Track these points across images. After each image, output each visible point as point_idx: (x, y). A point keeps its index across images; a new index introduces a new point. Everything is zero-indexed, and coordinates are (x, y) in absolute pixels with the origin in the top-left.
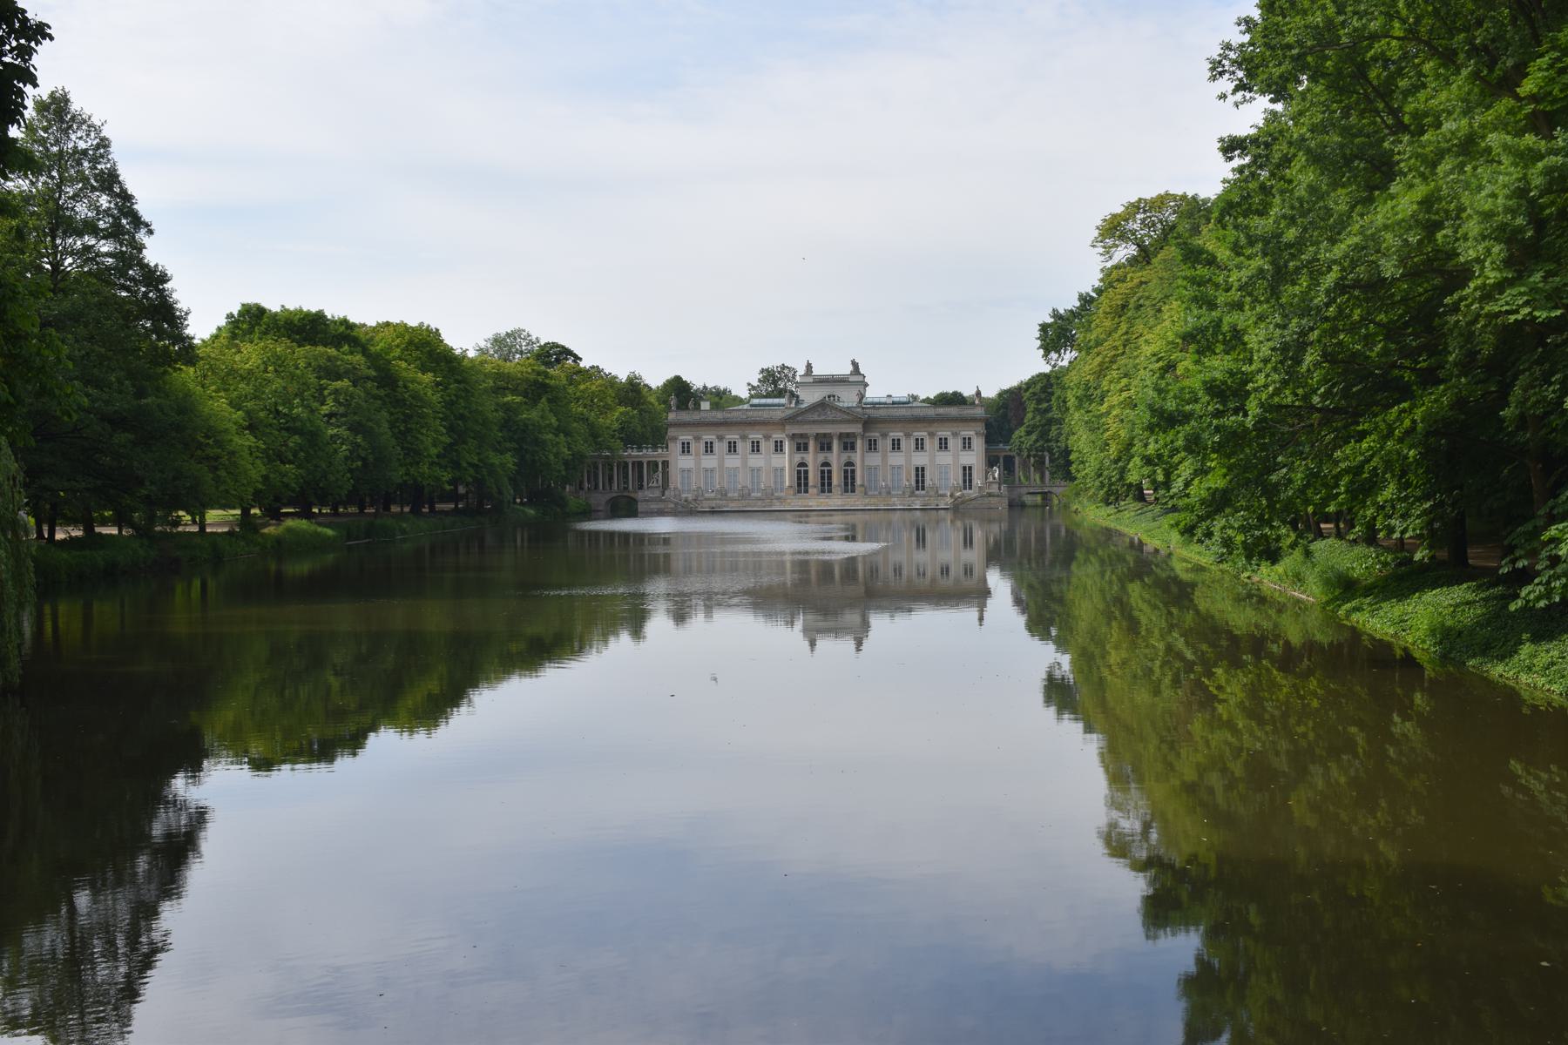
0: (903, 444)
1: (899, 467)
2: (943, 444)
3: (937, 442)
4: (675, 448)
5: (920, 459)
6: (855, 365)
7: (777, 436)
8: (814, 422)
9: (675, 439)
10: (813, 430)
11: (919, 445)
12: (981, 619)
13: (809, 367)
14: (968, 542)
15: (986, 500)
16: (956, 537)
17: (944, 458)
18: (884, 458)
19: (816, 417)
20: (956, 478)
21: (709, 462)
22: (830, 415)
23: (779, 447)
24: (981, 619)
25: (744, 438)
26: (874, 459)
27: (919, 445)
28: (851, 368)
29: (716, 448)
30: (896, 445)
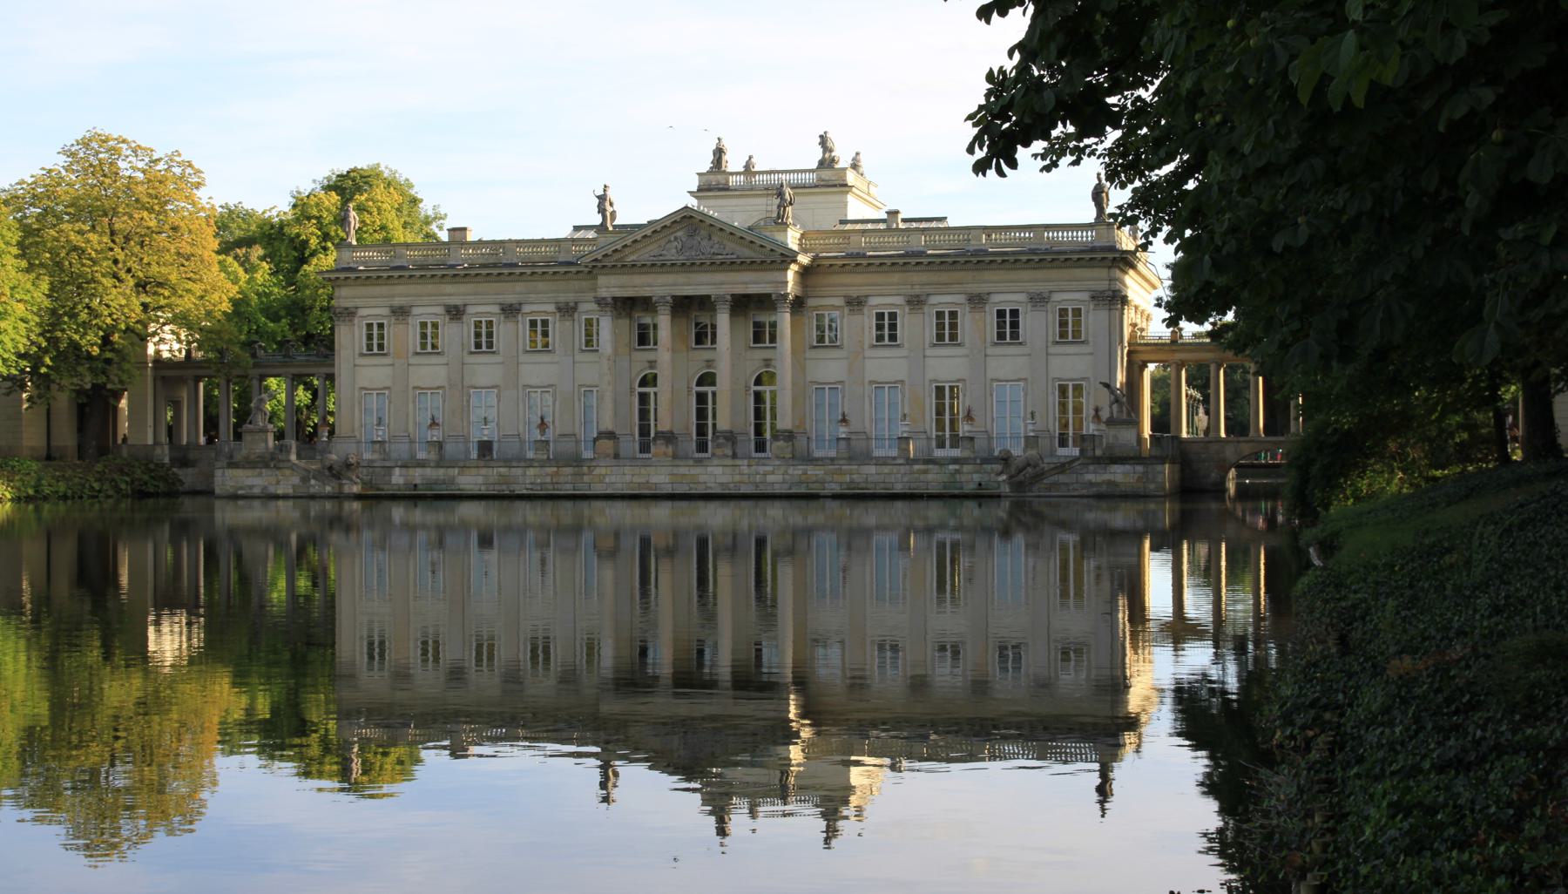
1: (895, 385)
2: (1008, 326)
4: (349, 339)
5: (947, 365)
6: (823, 140)
9: (350, 314)
10: (661, 286)
12: (1104, 791)
13: (719, 152)
17: (1007, 363)
19: (671, 254)
21: (430, 372)
24: (1104, 791)
26: (828, 367)
27: (947, 331)
28: (818, 153)
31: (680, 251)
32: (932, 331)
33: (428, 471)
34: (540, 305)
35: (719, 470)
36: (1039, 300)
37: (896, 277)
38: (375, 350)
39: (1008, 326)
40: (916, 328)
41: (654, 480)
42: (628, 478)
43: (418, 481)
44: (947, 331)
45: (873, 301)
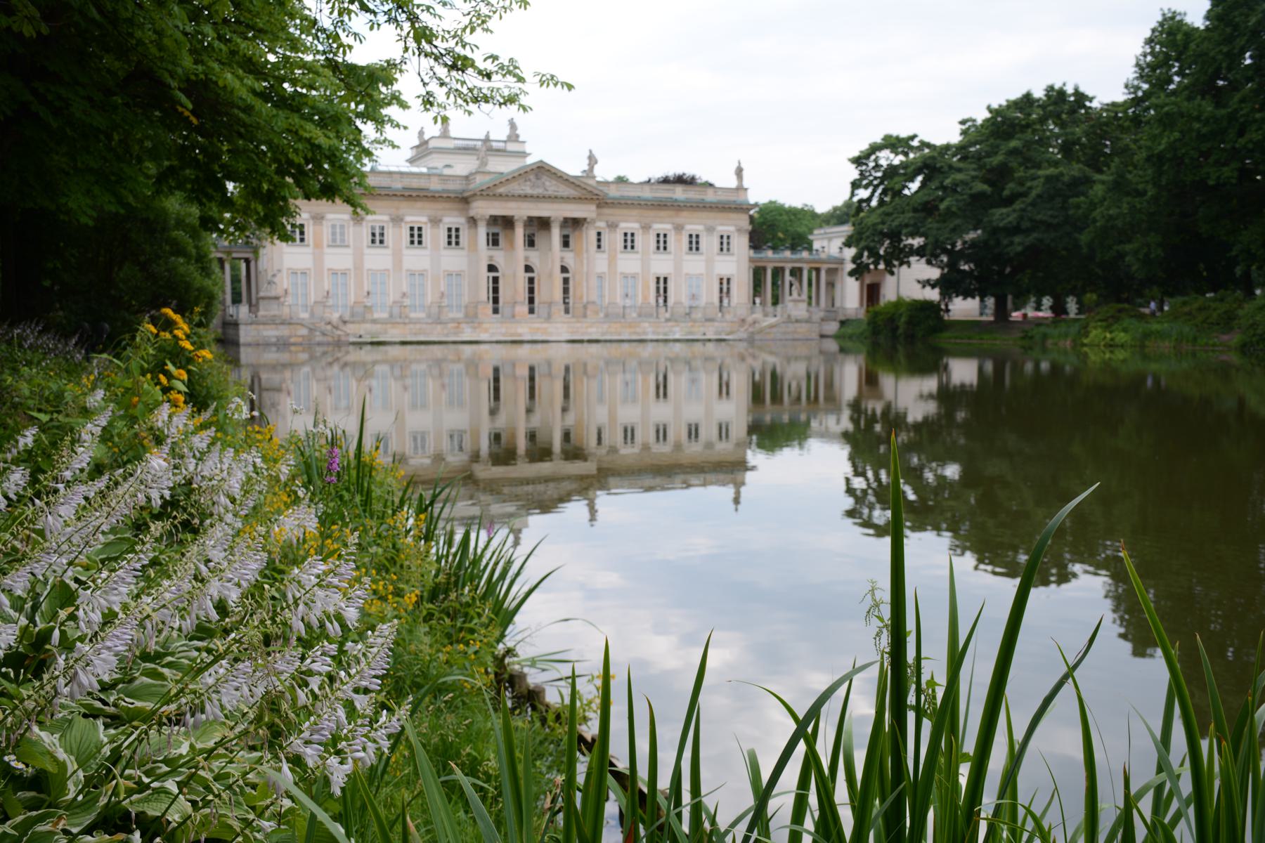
0: (639, 240)
1: (634, 277)
2: (694, 244)
3: (685, 240)
5: (661, 265)
7: (454, 219)
8: (525, 197)
10: (521, 211)
11: (662, 243)
12: (737, 501)
14: (724, 389)
15: (791, 327)
16: (709, 382)
17: (694, 264)
18: (612, 262)
19: (528, 190)
20: (710, 295)
22: (552, 187)
23: (453, 238)
24: (737, 501)
25: (397, 220)
26: (600, 263)
29: (389, 238)
30: (629, 242)
31: (533, 186)
32: (653, 244)
33: (368, 326)
34: (416, 216)
35: (559, 325)
36: (710, 230)
37: (635, 212)
38: (338, 243)
39: (694, 244)
40: (646, 242)
41: (520, 330)
42: (503, 330)
43: (362, 333)
44: (662, 243)
45: (623, 225)
